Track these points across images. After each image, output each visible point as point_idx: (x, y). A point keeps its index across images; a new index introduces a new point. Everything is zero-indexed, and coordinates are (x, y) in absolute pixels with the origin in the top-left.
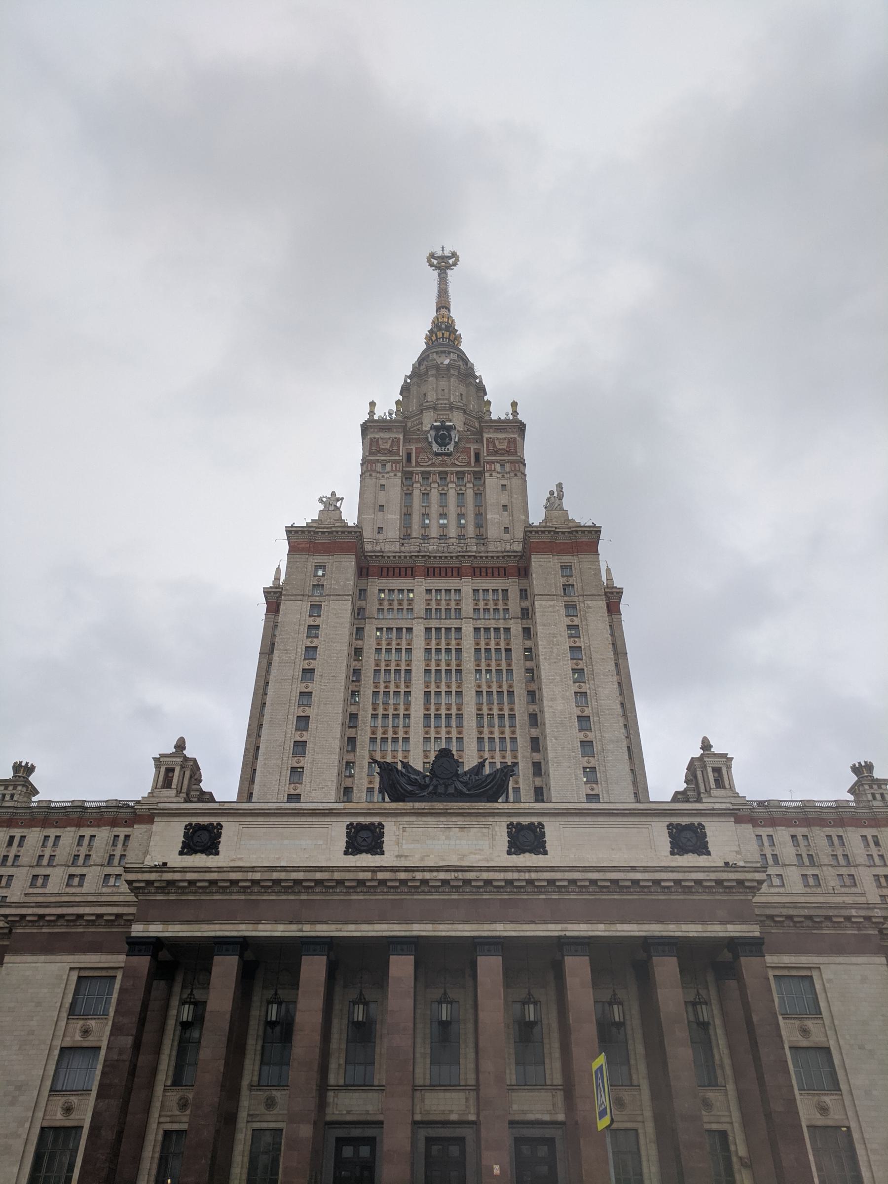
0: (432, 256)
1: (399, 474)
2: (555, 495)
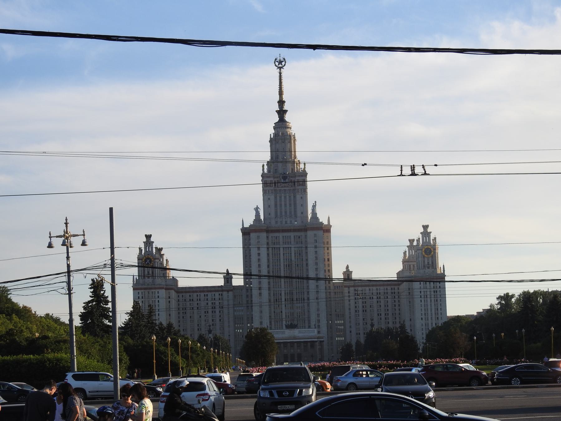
0: (276, 59)
1: (273, 194)
2: (314, 205)
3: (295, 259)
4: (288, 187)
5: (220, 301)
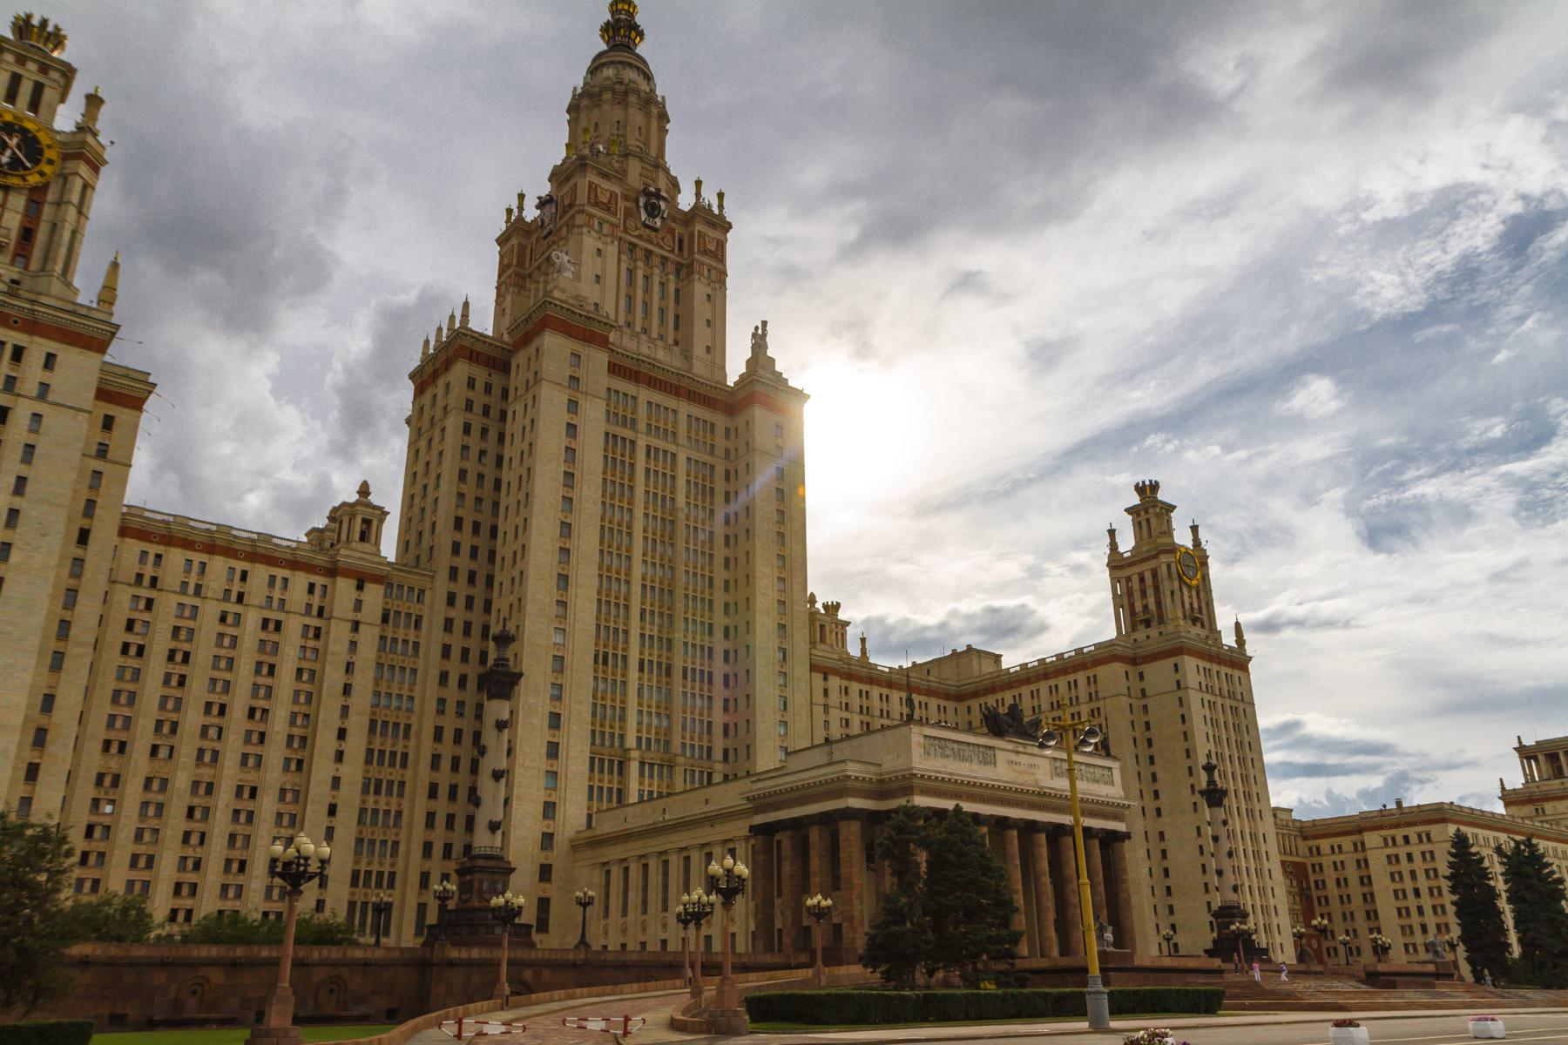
2: (760, 332)
3: (688, 504)
4: (661, 247)
5: (307, 621)
